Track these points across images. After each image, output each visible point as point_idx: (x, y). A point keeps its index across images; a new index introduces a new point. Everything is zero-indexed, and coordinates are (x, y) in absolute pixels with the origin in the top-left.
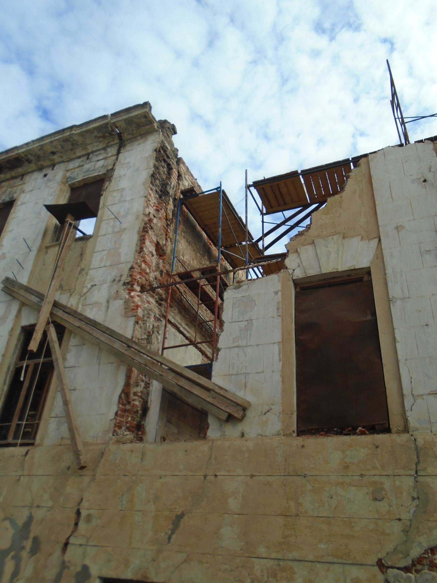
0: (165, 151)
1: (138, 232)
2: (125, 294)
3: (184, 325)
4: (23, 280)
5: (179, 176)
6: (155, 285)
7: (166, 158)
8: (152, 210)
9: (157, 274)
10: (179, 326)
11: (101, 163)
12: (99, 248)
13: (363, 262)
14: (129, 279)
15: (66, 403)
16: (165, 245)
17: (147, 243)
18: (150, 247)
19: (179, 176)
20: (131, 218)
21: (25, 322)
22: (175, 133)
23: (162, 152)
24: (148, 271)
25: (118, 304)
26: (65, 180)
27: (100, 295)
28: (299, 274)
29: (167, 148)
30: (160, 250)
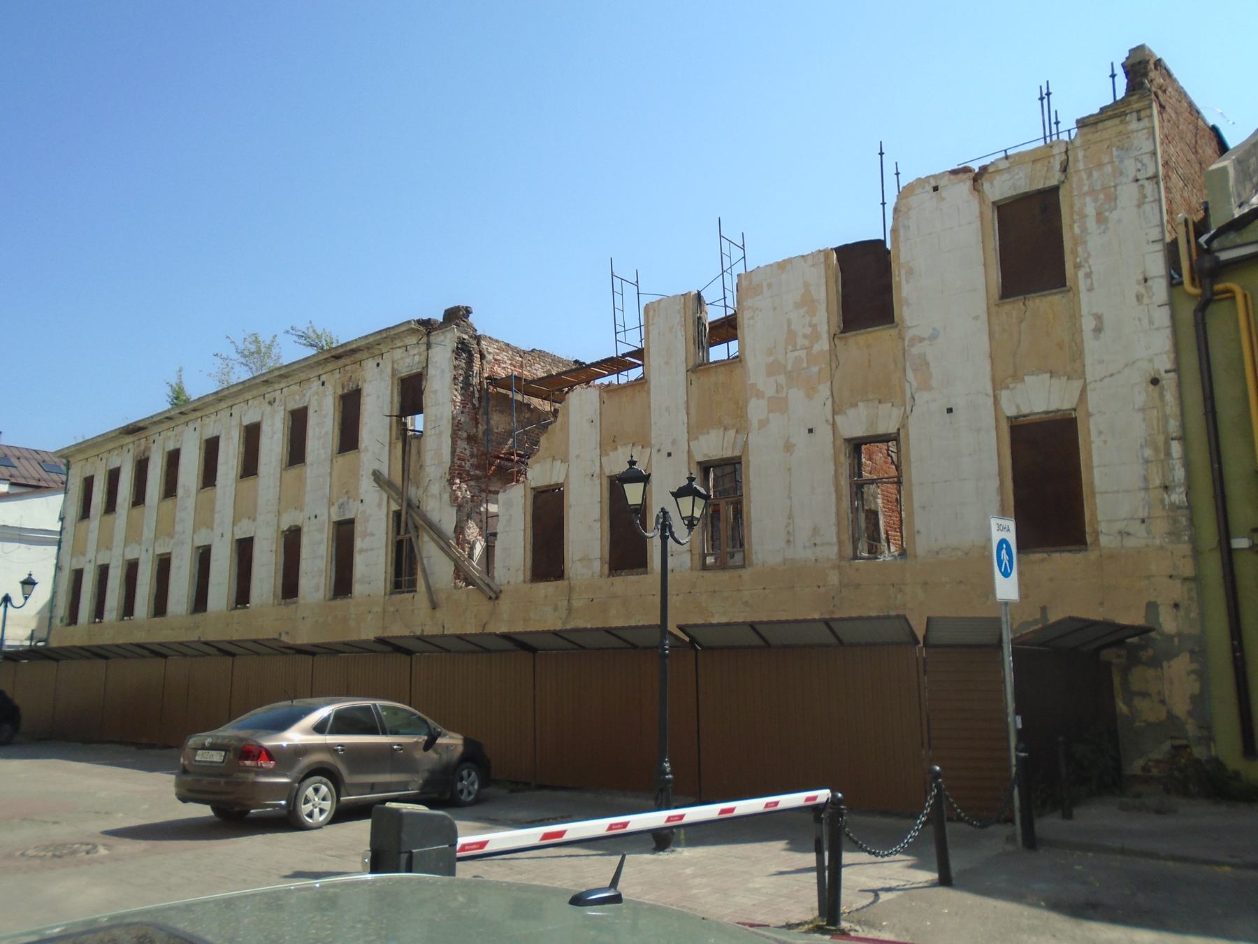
0: (463, 343)
2: (448, 489)
4: (385, 471)
5: (482, 357)
9: (474, 460)
11: (417, 358)
12: (428, 448)
13: (561, 481)
15: (424, 571)
17: (459, 442)
18: (462, 444)
19: (482, 357)
21: (395, 507)
25: (446, 496)
26: (394, 371)
27: (435, 489)
28: (533, 485)
30: (471, 439)
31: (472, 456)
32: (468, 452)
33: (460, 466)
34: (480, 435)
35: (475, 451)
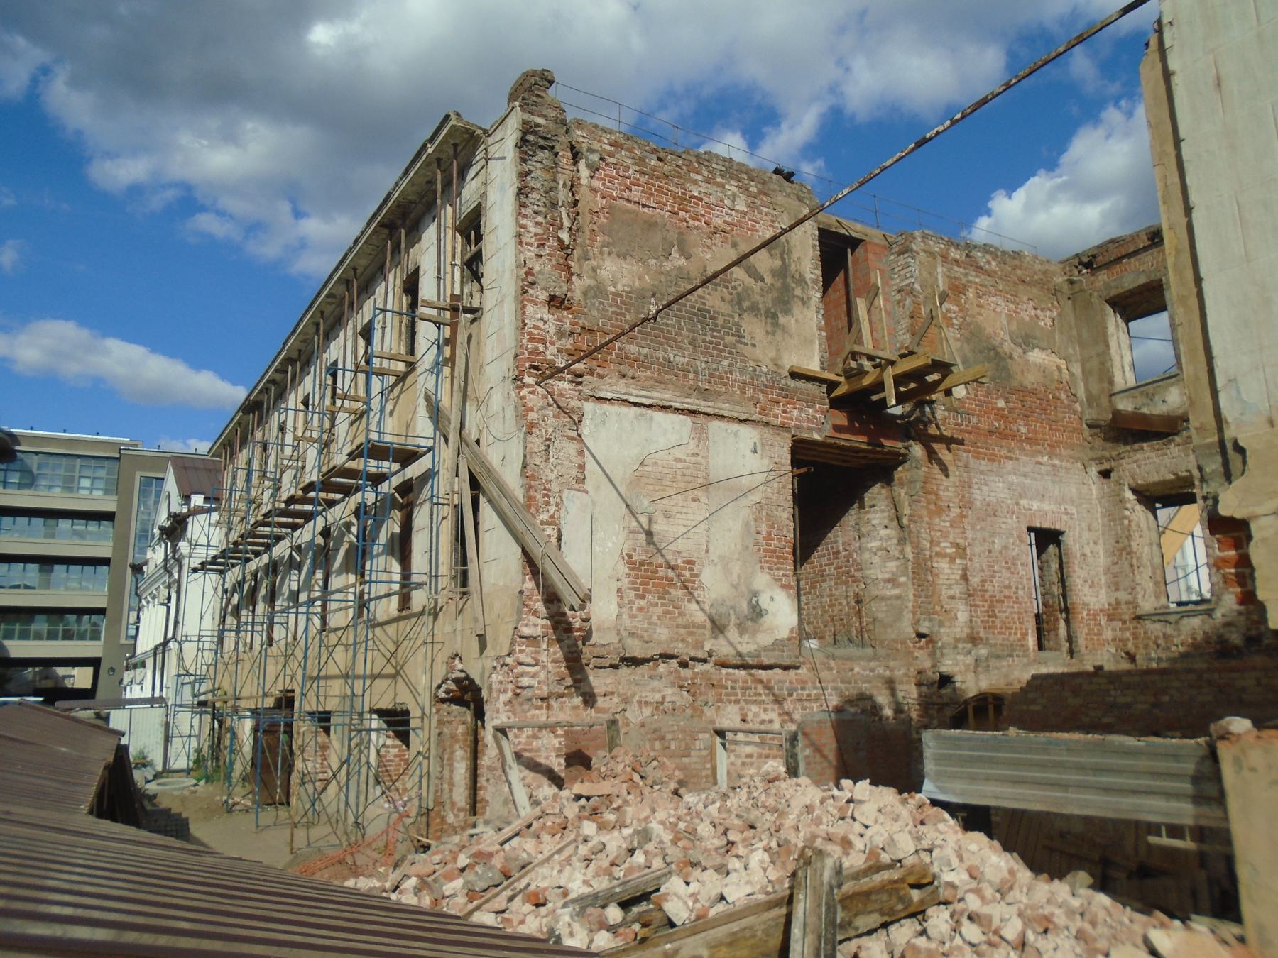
1: (516, 297)
2: (513, 394)
3: (635, 392)
6: (560, 363)
7: (542, 142)
8: (530, 253)
10: (625, 397)
14: (516, 373)
16: (569, 290)
17: (530, 308)
18: (538, 313)
20: (507, 275)
22: (551, 82)
23: (530, 137)
24: (541, 348)
25: (510, 412)
29: (538, 125)
31: (561, 334)
32: (552, 330)
33: (535, 352)
34: (577, 295)
35: (568, 326)
